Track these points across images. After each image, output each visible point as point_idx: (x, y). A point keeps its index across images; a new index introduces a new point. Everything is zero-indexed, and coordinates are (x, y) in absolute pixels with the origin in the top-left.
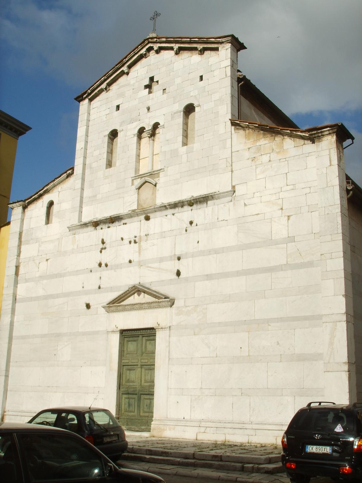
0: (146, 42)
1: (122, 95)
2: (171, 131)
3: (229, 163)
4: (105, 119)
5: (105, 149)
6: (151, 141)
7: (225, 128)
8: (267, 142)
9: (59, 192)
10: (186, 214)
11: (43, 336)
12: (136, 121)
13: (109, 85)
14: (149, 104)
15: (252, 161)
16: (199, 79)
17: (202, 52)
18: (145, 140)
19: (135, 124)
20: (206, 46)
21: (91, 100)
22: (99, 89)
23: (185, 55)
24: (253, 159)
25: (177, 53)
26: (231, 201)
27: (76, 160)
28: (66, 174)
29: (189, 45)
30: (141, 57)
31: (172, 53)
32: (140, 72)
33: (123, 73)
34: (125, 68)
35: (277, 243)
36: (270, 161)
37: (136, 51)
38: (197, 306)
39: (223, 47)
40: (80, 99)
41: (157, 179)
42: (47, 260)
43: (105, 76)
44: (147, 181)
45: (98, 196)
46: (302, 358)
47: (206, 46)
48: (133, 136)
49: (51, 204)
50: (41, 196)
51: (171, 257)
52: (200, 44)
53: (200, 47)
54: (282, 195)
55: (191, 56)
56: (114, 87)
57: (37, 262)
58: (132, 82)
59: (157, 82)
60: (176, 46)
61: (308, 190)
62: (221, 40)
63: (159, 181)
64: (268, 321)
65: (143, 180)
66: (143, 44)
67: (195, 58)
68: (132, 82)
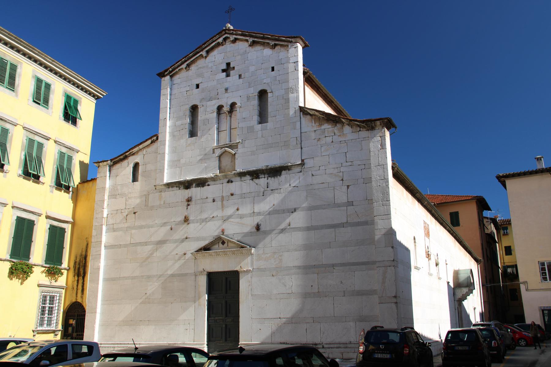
0: (224, 32)
1: (200, 75)
2: (248, 111)
4: (186, 95)
5: (188, 120)
8: (330, 126)
10: (263, 181)
11: (133, 278)
12: (215, 99)
14: (227, 85)
16: (271, 70)
18: (223, 116)
19: (214, 102)
20: (277, 43)
21: (171, 77)
22: (179, 68)
23: (258, 48)
24: (319, 140)
25: (250, 46)
26: (301, 172)
27: (160, 128)
30: (219, 45)
31: (246, 44)
32: (218, 57)
34: (204, 53)
35: (339, 206)
37: (215, 39)
38: (274, 253)
40: (162, 75)
42: (135, 213)
43: (185, 57)
45: (181, 160)
46: (360, 293)
47: (277, 43)
49: (136, 166)
50: (126, 158)
51: (251, 214)
53: (272, 43)
57: (125, 214)
58: (210, 65)
59: (234, 68)
60: (251, 40)
61: (363, 167)
64: (333, 266)
66: (220, 34)
68: (210, 65)
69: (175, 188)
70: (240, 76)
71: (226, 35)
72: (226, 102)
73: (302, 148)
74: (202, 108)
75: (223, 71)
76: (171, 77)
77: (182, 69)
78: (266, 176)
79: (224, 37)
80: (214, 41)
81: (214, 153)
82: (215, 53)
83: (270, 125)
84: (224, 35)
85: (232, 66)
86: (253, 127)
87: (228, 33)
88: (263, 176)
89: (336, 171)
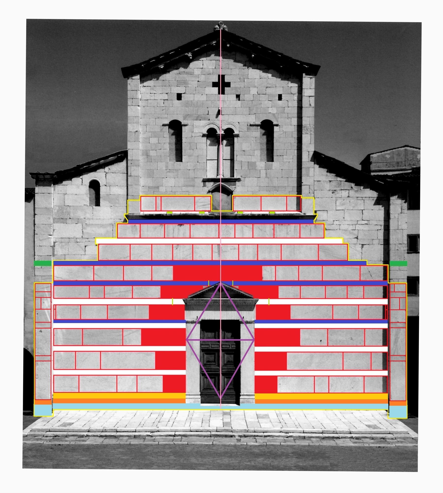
9: (107, 173)
12: (205, 119)
14: (221, 105)
15: (333, 193)
16: (277, 98)
19: (203, 122)
36: (349, 197)
41: (234, 187)
44: (223, 187)
45: (160, 188)
48: (202, 135)
54: (358, 227)
57: (83, 246)
58: (197, 72)
70: (238, 96)
74: (186, 127)
75: (215, 85)
83: (275, 164)
89: (351, 228)
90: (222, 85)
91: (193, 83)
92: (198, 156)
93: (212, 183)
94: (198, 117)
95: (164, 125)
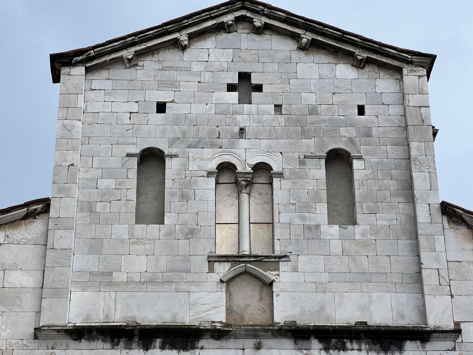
1: (173, 85)
3: (445, 280)
6: (245, 197)
7: (428, 214)
12: (212, 145)
13: (138, 55)
17: (362, 64)
19: (208, 152)
20: (374, 56)
25: (302, 48)
26: (454, 349)
28: (26, 209)
29: (337, 43)
31: (291, 45)
33: (176, 44)
34: (183, 37)
39: (412, 71)
45: (115, 274)
47: (374, 56)
48: (205, 174)
52: (361, 50)
53: (362, 55)
55: (336, 64)
56: (149, 64)
58: (196, 68)
60: (307, 37)
62: (410, 57)
63: (277, 276)
65: (239, 268)
67: (344, 71)
69: (99, 344)
70: (278, 107)
71: (243, 13)
72: (245, 156)
73: (452, 296)
74: (175, 160)
75: (231, 88)
76: (88, 70)
77: (121, 59)
78: (363, 347)
79: (238, 14)
80: (212, 18)
81: (211, 270)
82: (209, 43)
84: (237, 10)
85: (255, 80)
86: (318, 227)
87: (248, 10)
88: (355, 346)
90: (245, 85)
91: (189, 85)
92: (197, 213)
93: (227, 266)
94: (198, 143)
95: (128, 155)
